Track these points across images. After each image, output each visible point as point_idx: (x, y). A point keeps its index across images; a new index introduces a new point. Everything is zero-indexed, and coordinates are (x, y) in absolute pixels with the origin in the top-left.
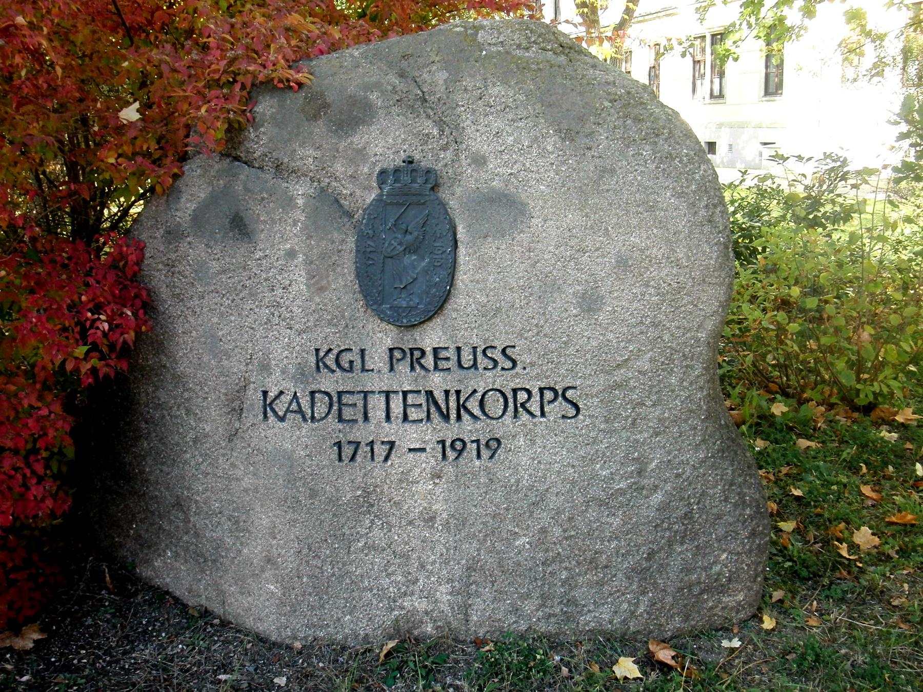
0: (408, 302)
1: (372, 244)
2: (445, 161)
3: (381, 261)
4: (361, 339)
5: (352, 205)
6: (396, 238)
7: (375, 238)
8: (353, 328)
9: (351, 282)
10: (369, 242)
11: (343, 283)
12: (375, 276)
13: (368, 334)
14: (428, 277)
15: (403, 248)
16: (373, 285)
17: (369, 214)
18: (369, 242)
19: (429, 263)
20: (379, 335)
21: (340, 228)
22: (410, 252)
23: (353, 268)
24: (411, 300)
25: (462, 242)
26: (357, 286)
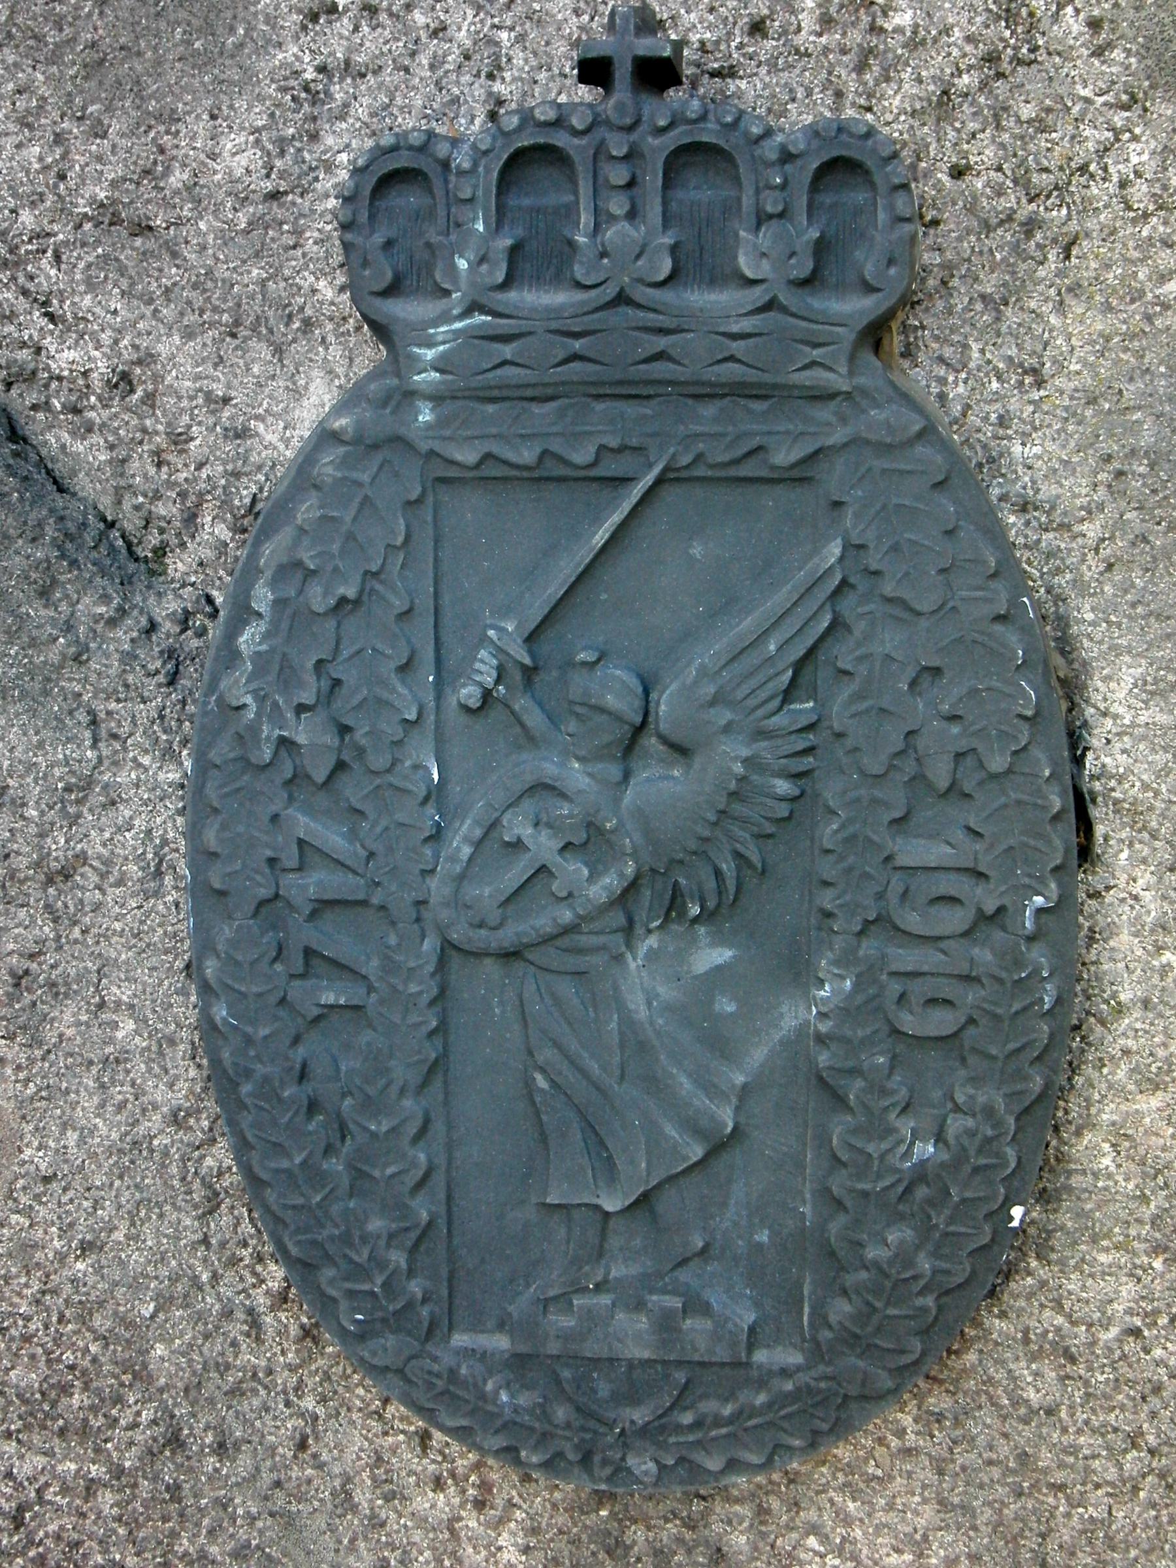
0: (666, 1325)
1: (334, 838)
2: (936, 64)
3: (422, 988)
4: (288, 1521)
5: (140, 467)
6: (543, 788)
7: (353, 790)
8: (220, 1449)
9: (176, 1119)
10: (303, 824)
11: (107, 1131)
12: (370, 1105)
13: (345, 1500)
14: (839, 1129)
15: (610, 883)
16: (359, 1175)
17: (291, 568)
18: (303, 824)
19: (846, 1011)
20: (442, 1503)
21: (49, 678)
22: (674, 906)
23: (186, 1010)
24: (695, 1305)
25: (1135, 814)
26: (220, 1155)
